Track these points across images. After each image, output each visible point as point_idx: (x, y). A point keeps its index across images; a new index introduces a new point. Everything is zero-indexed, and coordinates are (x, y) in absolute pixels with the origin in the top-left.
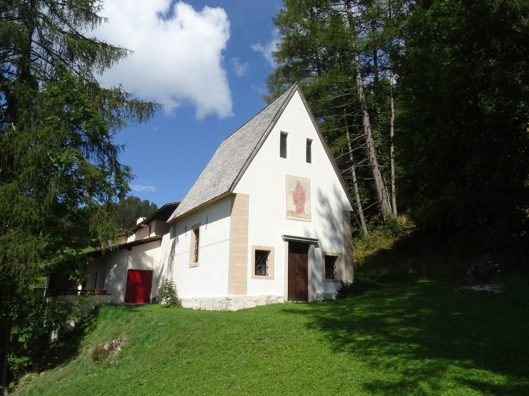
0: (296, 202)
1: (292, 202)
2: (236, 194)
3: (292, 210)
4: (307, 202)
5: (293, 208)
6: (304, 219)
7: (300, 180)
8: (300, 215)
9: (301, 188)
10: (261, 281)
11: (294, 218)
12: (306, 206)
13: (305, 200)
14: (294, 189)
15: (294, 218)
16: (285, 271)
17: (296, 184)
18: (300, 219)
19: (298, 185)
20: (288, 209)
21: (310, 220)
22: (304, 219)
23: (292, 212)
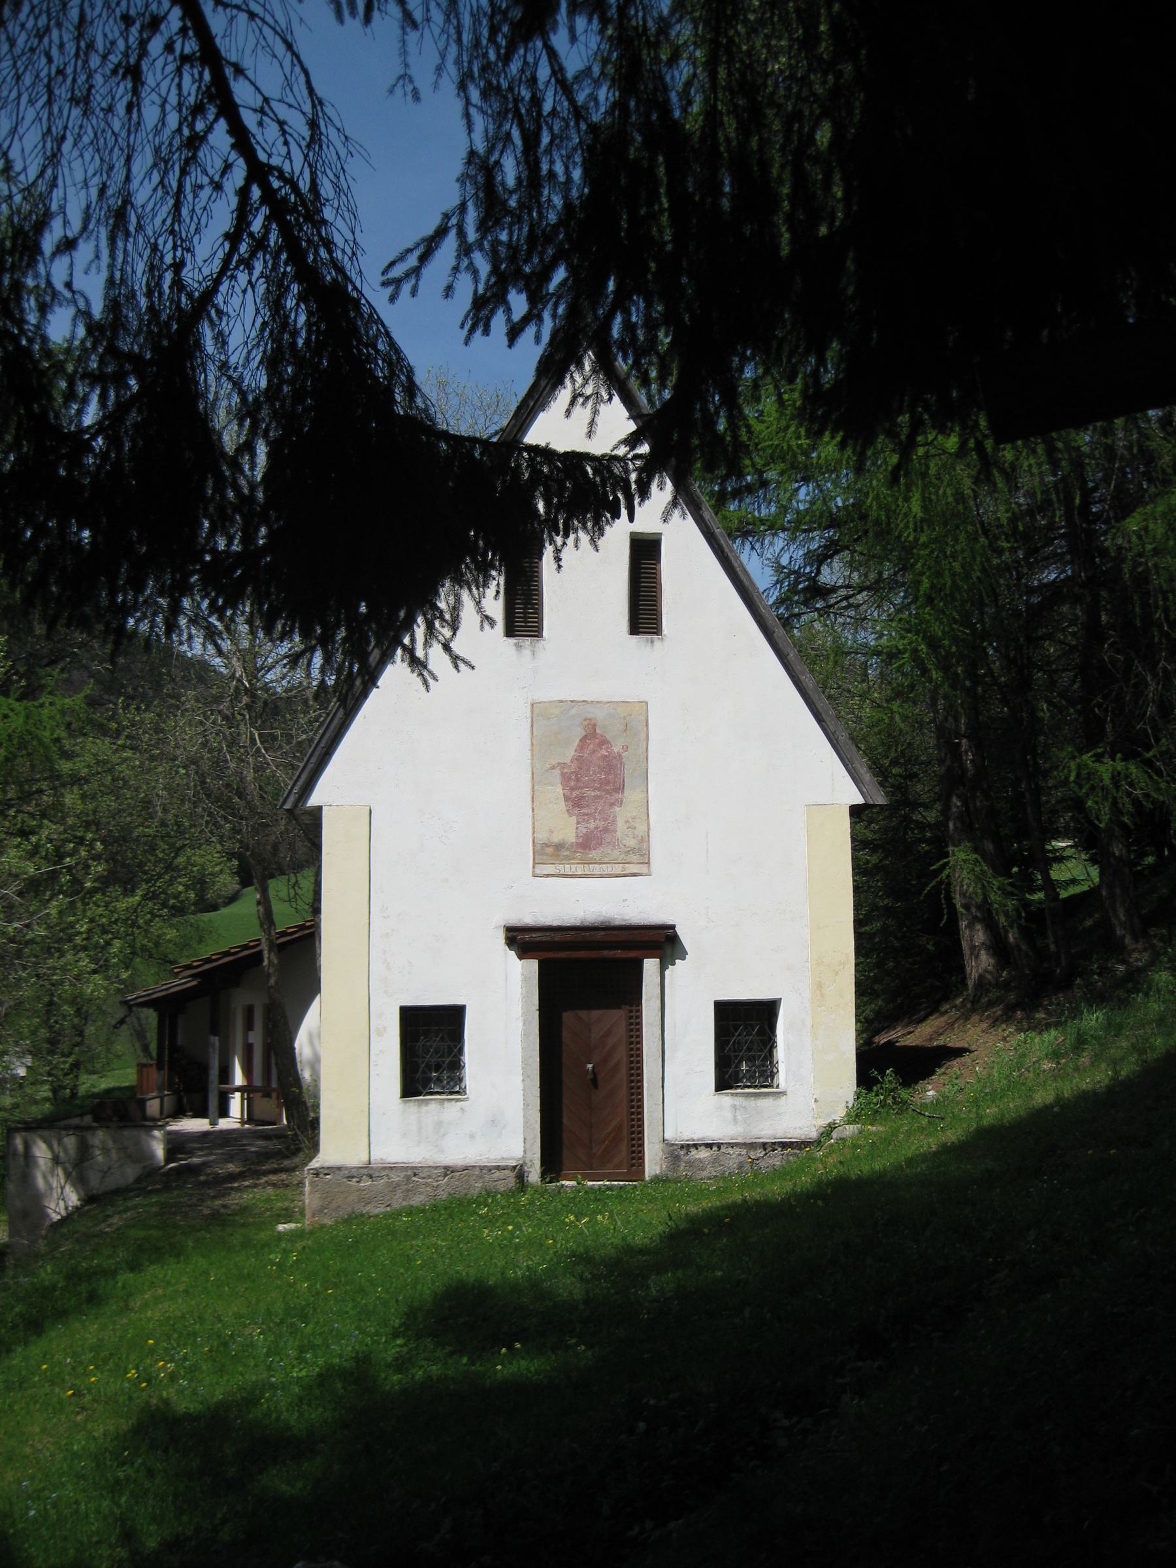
0: (576, 803)
1: (562, 805)
2: (319, 809)
3: (556, 839)
4: (631, 795)
5: (567, 829)
6: (618, 869)
7: (599, 714)
8: (594, 854)
9: (604, 742)
10: (434, 1110)
11: (568, 869)
12: (622, 815)
13: (620, 789)
14: (569, 753)
15: (568, 869)
16: (526, 1077)
17: (579, 733)
18: (596, 869)
19: (592, 736)
20: (542, 837)
21: (643, 869)
22: (618, 869)
23: (559, 847)
